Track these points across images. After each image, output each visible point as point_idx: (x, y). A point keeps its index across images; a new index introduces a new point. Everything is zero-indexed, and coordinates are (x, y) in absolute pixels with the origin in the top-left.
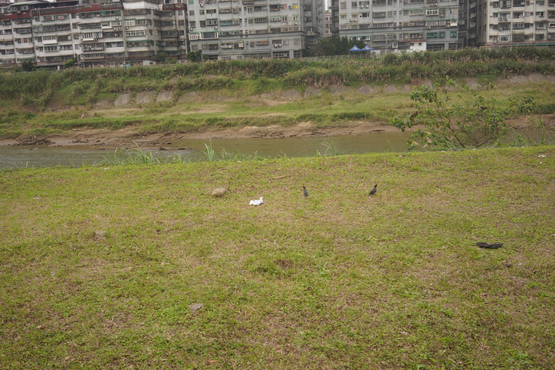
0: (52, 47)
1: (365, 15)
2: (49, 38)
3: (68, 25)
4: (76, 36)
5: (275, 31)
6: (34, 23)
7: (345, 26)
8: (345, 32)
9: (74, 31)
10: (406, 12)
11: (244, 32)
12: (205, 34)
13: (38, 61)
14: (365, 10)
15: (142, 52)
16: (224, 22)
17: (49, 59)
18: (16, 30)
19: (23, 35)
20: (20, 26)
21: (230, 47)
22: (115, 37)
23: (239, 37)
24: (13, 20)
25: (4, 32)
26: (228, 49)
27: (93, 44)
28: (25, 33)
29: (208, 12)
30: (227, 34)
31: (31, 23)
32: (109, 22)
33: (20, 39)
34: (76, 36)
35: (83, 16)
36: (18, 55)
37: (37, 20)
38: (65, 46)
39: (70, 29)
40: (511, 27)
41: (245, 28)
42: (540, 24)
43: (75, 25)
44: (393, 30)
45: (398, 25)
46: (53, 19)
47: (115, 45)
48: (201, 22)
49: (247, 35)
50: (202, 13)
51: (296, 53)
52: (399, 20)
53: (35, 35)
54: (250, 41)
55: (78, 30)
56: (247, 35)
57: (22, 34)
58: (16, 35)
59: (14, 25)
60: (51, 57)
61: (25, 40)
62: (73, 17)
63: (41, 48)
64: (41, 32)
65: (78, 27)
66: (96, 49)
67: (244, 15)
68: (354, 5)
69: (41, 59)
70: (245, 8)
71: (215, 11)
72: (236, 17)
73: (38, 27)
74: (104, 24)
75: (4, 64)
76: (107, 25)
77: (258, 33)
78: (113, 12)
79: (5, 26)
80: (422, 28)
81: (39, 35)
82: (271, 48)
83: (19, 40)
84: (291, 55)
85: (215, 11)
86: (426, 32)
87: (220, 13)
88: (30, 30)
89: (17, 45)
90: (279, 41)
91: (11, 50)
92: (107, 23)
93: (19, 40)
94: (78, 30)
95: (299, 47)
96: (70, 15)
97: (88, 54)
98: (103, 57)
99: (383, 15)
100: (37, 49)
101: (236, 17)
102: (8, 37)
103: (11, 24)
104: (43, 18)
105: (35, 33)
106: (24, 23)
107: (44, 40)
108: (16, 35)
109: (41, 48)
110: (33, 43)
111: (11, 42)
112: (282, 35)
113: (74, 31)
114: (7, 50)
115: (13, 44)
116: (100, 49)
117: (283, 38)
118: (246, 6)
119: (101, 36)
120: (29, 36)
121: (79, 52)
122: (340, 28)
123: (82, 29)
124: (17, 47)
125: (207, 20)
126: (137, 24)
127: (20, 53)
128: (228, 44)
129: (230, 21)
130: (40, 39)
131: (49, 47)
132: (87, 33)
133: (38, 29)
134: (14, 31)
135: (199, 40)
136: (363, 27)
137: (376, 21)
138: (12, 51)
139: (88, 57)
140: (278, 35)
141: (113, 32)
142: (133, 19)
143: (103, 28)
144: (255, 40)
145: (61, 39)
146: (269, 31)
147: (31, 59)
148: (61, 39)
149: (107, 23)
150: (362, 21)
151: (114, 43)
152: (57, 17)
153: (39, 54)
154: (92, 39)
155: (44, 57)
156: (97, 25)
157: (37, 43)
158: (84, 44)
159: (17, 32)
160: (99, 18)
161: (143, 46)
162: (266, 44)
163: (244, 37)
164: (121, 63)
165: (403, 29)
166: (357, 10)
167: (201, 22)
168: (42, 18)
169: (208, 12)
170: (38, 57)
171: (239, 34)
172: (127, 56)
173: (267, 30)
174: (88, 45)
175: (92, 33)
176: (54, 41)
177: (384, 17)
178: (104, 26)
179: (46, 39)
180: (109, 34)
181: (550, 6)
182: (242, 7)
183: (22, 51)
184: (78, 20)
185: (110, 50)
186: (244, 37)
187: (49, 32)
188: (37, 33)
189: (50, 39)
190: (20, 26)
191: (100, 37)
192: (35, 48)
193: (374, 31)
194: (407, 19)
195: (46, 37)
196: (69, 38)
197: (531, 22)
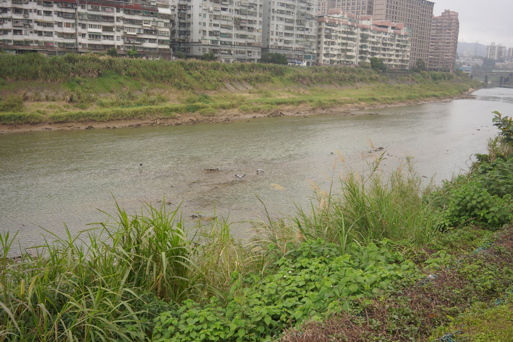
0: (97, 36)
1: (281, 41)
2: (95, 27)
3: (112, 18)
4: (119, 29)
5: (249, 44)
6: (79, 9)
7: (271, 46)
8: (272, 50)
9: (117, 24)
10: (297, 42)
11: (233, 43)
12: (213, 41)
13: (80, 47)
14: (281, 38)
15: (165, 49)
16: (224, 34)
17: (93, 47)
18: (59, 14)
19: (66, 19)
20: (64, 10)
21: (226, 52)
22: (152, 34)
23: (230, 46)
24: (55, 2)
25: (42, 12)
26: (225, 53)
27: (134, 37)
28: (70, 18)
29: (215, 25)
30: (225, 43)
31: (76, 9)
32: (150, 21)
33: (61, 23)
34: (119, 29)
35: (128, 11)
36: (56, 39)
37: (83, 7)
38: (107, 36)
39: (113, 22)
40: (330, 56)
41: (234, 40)
42: (339, 55)
43: (118, 18)
44: (291, 51)
45: (294, 49)
46: (100, 9)
47: (148, 41)
48: (209, 31)
49: (234, 46)
50: (210, 24)
51: (258, 60)
52: (294, 46)
53: (79, 21)
54: (236, 49)
55: (121, 24)
56: (234, 46)
57: (65, 18)
58: (55, 18)
59: (55, 8)
60: (95, 45)
61: (68, 25)
62: (118, 11)
63: (83, 35)
64: (86, 20)
65: (122, 22)
66: (135, 43)
67: (234, 31)
68: (277, 33)
69: (84, 45)
70: (235, 26)
71: (218, 25)
72: (229, 32)
73: (82, 14)
74: (145, 22)
75: (39, 46)
76: (147, 24)
77: (240, 44)
78: (152, 13)
79: (46, 7)
80: (302, 52)
81: (83, 22)
82: (246, 56)
83: (60, 24)
84: (256, 61)
85: (218, 25)
86: (304, 54)
87: (221, 27)
88: (73, 16)
89: (56, 28)
90: (249, 52)
91: (49, 32)
92: (148, 22)
93: (60, 24)
94: (121, 24)
95: (259, 57)
96: (115, 9)
97: (130, 46)
98: (141, 50)
99: (288, 42)
100: (80, 35)
101: (229, 32)
102: (47, 19)
103: (52, 6)
104: (91, 7)
105: (79, 19)
106: (69, 8)
107: (89, 27)
108: (55, 18)
109: (83, 35)
110: (76, 29)
111: (49, 25)
112: (252, 48)
113: (117, 24)
114: (45, 32)
115: (53, 27)
116: (139, 43)
117: (253, 50)
118: (236, 25)
119: (142, 32)
120: (73, 21)
121: (120, 43)
122: (270, 47)
123: (125, 23)
124: (56, 31)
125: (215, 31)
126: (165, 26)
127: (58, 37)
128: (225, 50)
129: (226, 34)
130: (84, 26)
131: (93, 35)
132: (131, 28)
133: (82, 17)
134: (55, 14)
135: (208, 45)
136: (280, 48)
137: (286, 45)
138: (50, 34)
139: (129, 48)
140: (250, 48)
141: (151, 30)
142: (163, 22)
143: (144, 25)
144: (238, 49)
145: (105, 29)
146: (246, 45)
147: (72, 44)
148: (105, 29)
149: (148, 22)
150: (280, 44)
151: (147, 39)
152: (104, 9)
153: (80, 40)
154: (135, 34)
155: (86, 44)
156: (139, 22)
157: (80, 30)
158: (126, 37)
159: (58, 16)
160: (142, 16)
161: (166, 44)
162: (243, 53)
163: (233, 46)
164: (157, 57)
165: (296, 52)
166: (278, 37)
167: (209, 31)
168: (90, 7)
169: (215, 25)
170: (80, 44)
171: (230, 44)
172: (157, 51)
173: (245, 44)
174: (132, 38)
175: (135, 28)
176: (100, 31)
177: (288, 43)
178: (145, 23)
179: (92, 27)
180: (282, 48)
181: (342, 46)
182: (233, 25)
183: (62, 35)
184: (121, 14)
185: (147, 45)
186: (233, 46)
187: (94, 21)
188: (82, 20)
189: (96, 28)
190: (64, 10)
191: (141, 32)
192: (78, 34)
193: (285, 51)
194: (297, 46)
195: (92, 25)
196: (114, 29)
197: (336, 54)
